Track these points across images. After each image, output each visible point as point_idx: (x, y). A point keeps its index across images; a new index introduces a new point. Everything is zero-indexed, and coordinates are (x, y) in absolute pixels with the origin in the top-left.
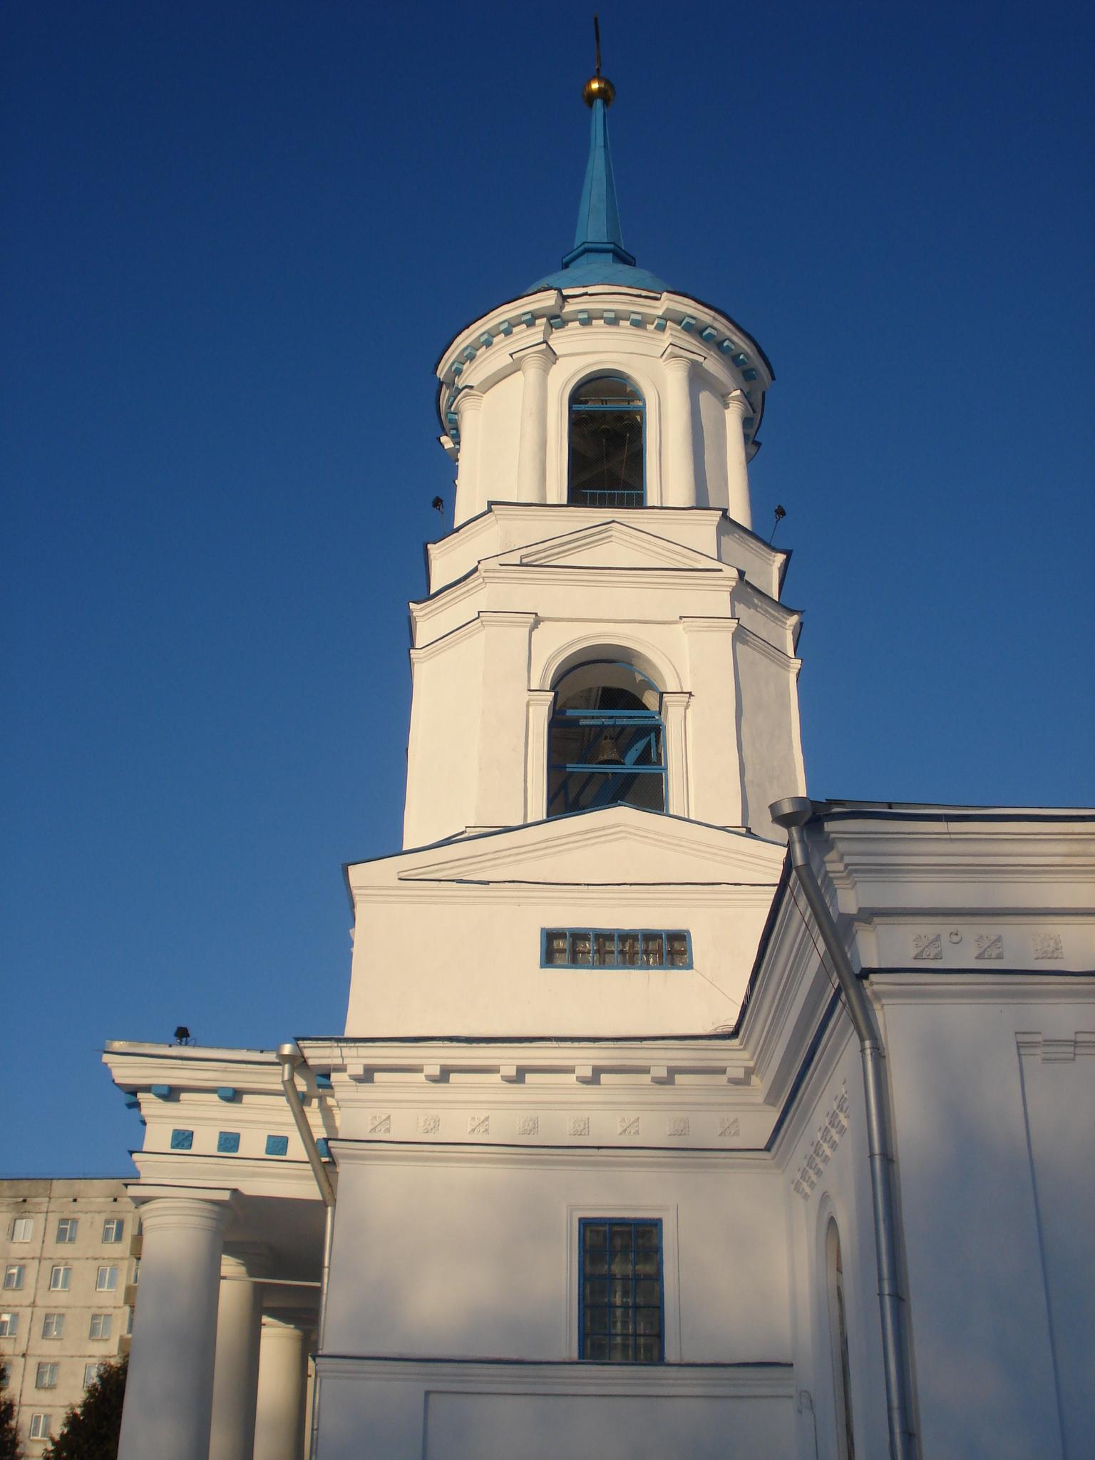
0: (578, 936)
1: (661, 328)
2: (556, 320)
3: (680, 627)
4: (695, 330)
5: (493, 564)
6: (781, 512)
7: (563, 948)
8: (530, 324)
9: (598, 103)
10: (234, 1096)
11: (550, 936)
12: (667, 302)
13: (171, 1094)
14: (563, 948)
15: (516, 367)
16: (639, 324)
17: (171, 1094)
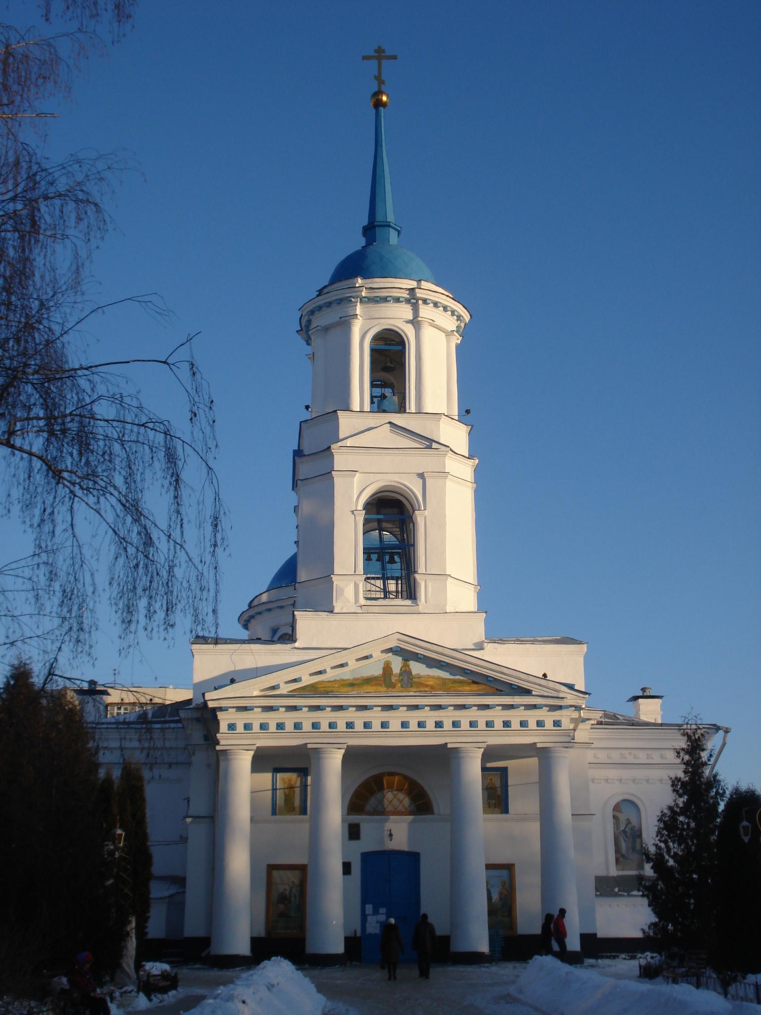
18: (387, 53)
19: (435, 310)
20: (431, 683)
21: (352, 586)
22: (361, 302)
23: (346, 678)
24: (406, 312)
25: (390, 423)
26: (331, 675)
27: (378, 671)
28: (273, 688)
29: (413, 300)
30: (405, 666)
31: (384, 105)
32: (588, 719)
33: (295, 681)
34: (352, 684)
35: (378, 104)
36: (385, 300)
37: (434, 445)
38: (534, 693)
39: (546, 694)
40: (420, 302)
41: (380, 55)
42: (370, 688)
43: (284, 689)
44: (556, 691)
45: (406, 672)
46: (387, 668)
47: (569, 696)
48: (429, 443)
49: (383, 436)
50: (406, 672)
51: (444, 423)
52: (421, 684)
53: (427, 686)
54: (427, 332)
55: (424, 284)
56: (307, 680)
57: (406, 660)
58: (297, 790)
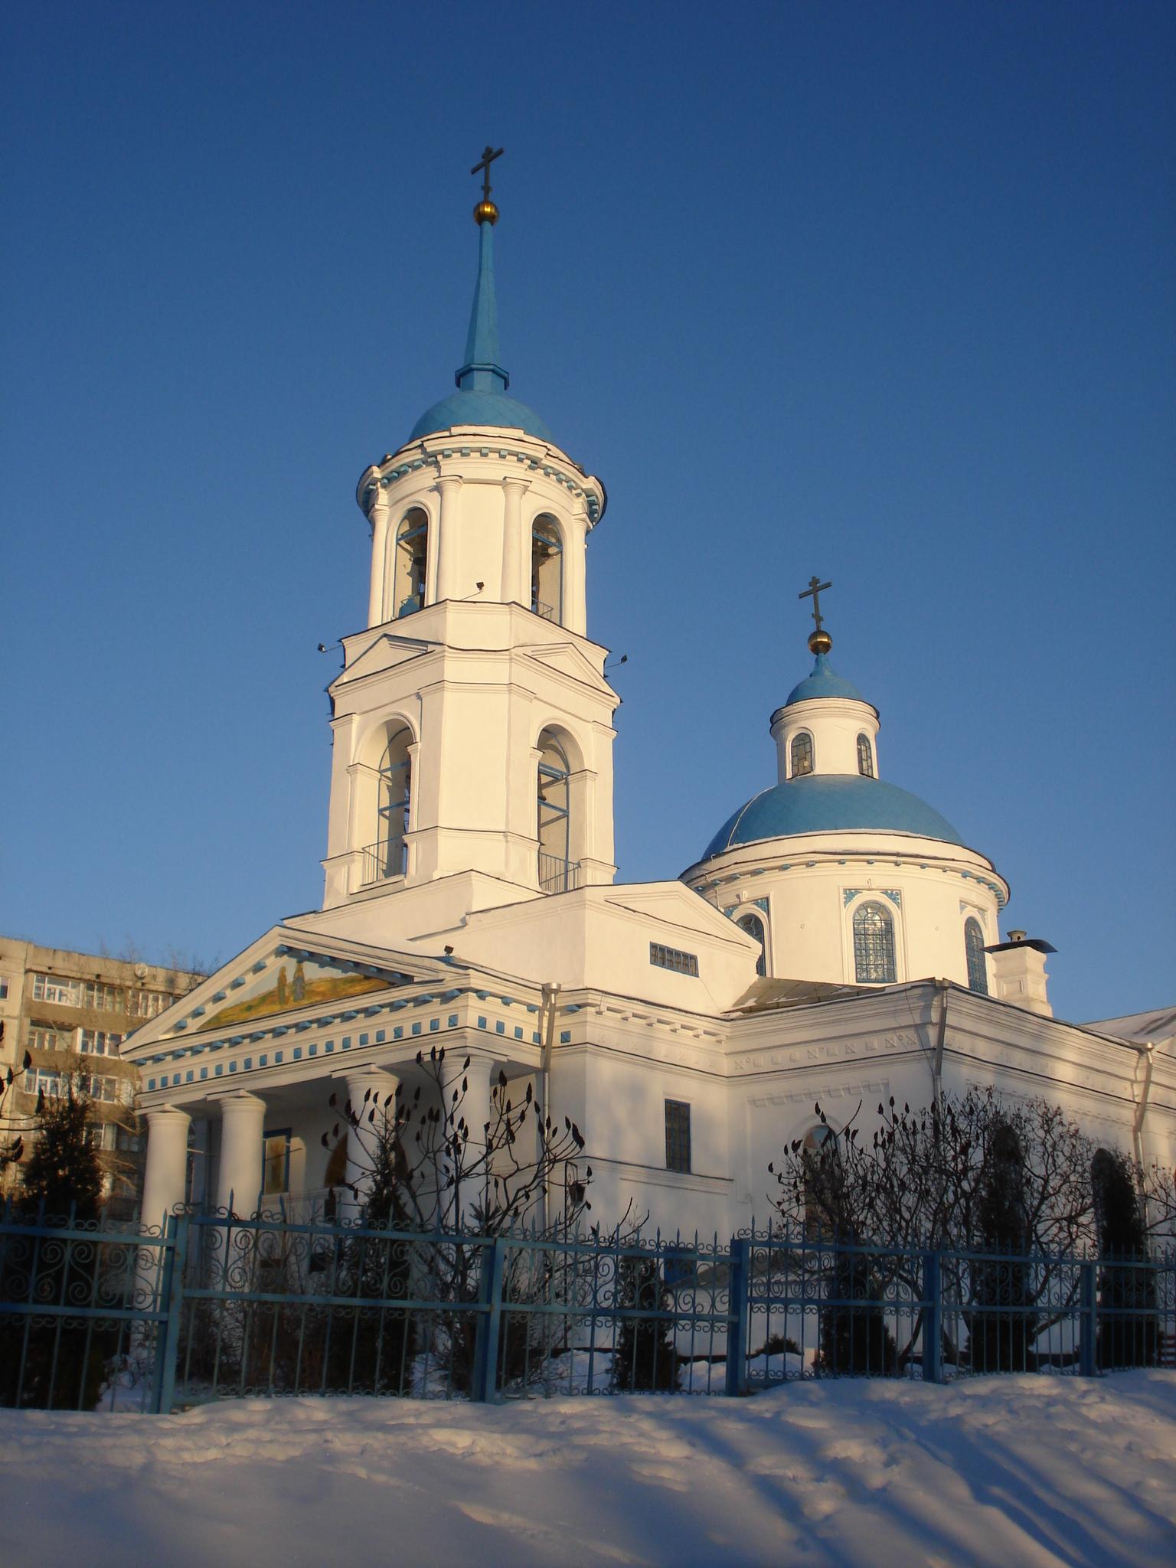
0: (662, 949)
1: (578, 495)
2: (535, 463)
3: (590, 726)
4: (591, 504)
5: (520, 651)
6: (624, 659)
7: (663, 956)
8: (520, 460)
9: (487, 224)
10: (506, 1001)
11: (653, 946)
12: (590, 483)
13: (481, 995)
14: (663, 956)
15: (504, 483)
16: (570, 488)
17: (481, 995)
18: (495, 151)
19: (465, 460)
20: (322, 989)
21: (344, 870)
22: (384, 486)
23: (247, 998)
24: (426, 477)
25: (385, 635)
26: (233, 997)
27: (273, 985)
28: (180, 1027)
29: (432, 460)
30: (300, 970)
31: (491, 218)
32: (580, 1006)
33: (197, 1014)
34: (250, 1008)
35: (481, 218)
36: (400, 474)
37: (431, 648)
38: (416, 980)
39: (427, 978)
40: (440, 457)
41: (490, 156)
42: (265, 1010)
43: (193, 1025)
44: (435, 971)
45: (299, 978)
46: (282, 979)
47: (448, 977)
48: (424, 648)
49: (386, 654)
50: (299, 978)
51: (452, 613)
52: (313, 993)
53: (318, 994)
54: (455, 495)
55: (455, 430)
56: (212, 1010)
57: (300, 962)
58: (283, 1158)
